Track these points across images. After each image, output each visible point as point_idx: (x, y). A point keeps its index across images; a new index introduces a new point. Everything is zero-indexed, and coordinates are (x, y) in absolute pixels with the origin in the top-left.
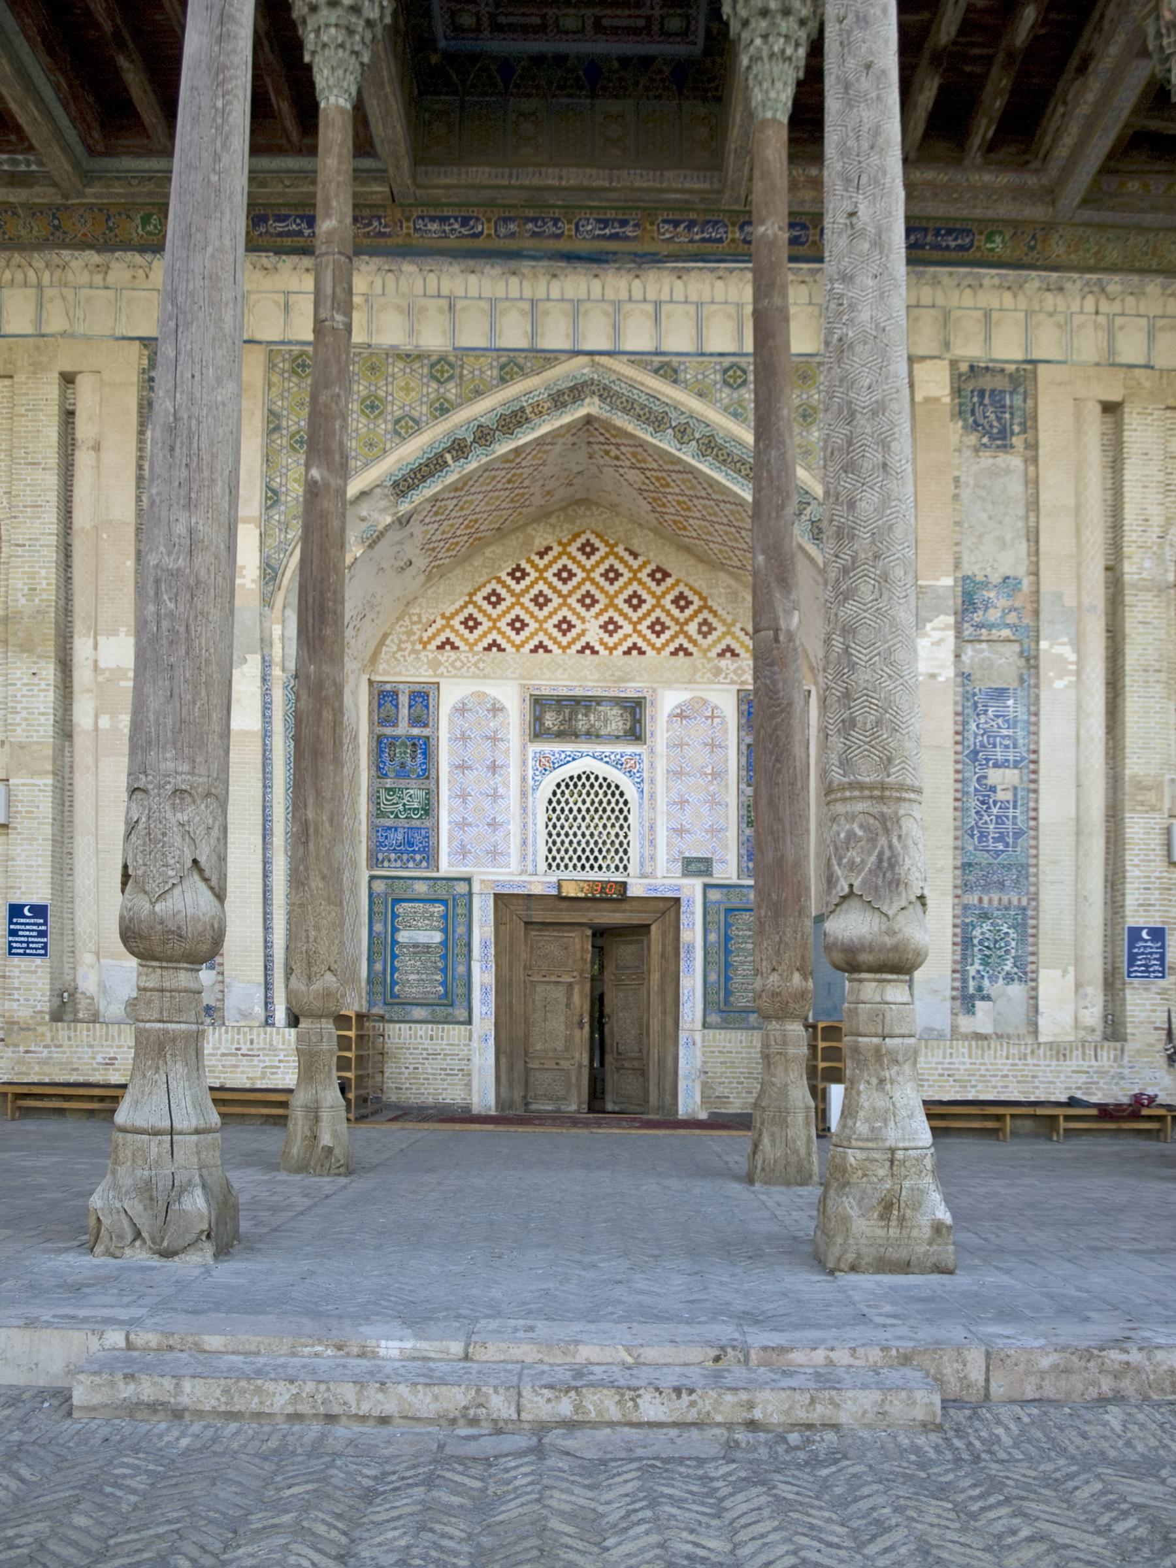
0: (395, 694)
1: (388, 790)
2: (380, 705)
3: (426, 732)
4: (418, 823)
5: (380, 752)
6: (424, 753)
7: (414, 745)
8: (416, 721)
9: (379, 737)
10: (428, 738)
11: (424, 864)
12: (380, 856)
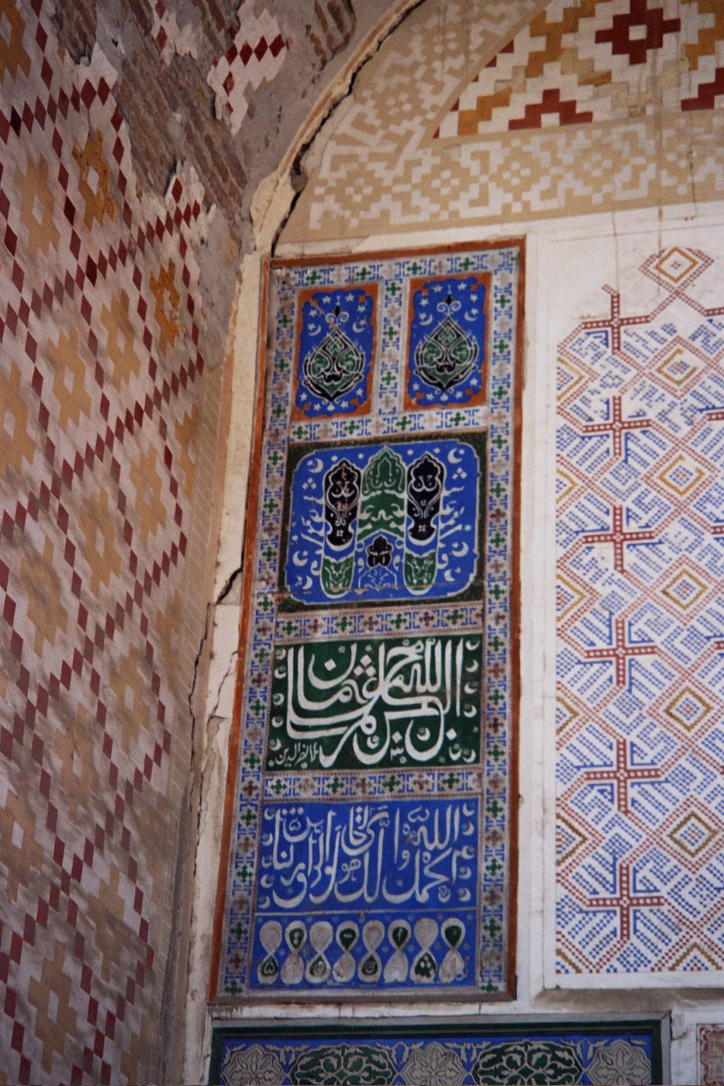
0: (360, 300)
1: (319, 652)
2: (305, 343)
3: (478, 417)
4: (432, 782)
5: (294, 505)
6: (461, 501)
7: (426, 470)
8: (437, 380)
9: (295, 453)
10: (478, 439)
11: (454, 963)
12: (271, 936)
